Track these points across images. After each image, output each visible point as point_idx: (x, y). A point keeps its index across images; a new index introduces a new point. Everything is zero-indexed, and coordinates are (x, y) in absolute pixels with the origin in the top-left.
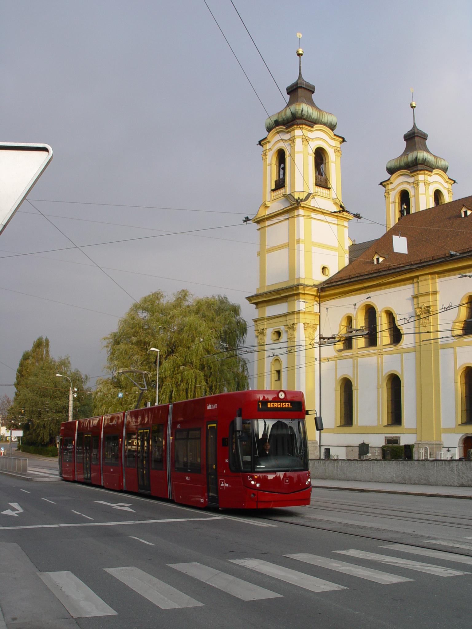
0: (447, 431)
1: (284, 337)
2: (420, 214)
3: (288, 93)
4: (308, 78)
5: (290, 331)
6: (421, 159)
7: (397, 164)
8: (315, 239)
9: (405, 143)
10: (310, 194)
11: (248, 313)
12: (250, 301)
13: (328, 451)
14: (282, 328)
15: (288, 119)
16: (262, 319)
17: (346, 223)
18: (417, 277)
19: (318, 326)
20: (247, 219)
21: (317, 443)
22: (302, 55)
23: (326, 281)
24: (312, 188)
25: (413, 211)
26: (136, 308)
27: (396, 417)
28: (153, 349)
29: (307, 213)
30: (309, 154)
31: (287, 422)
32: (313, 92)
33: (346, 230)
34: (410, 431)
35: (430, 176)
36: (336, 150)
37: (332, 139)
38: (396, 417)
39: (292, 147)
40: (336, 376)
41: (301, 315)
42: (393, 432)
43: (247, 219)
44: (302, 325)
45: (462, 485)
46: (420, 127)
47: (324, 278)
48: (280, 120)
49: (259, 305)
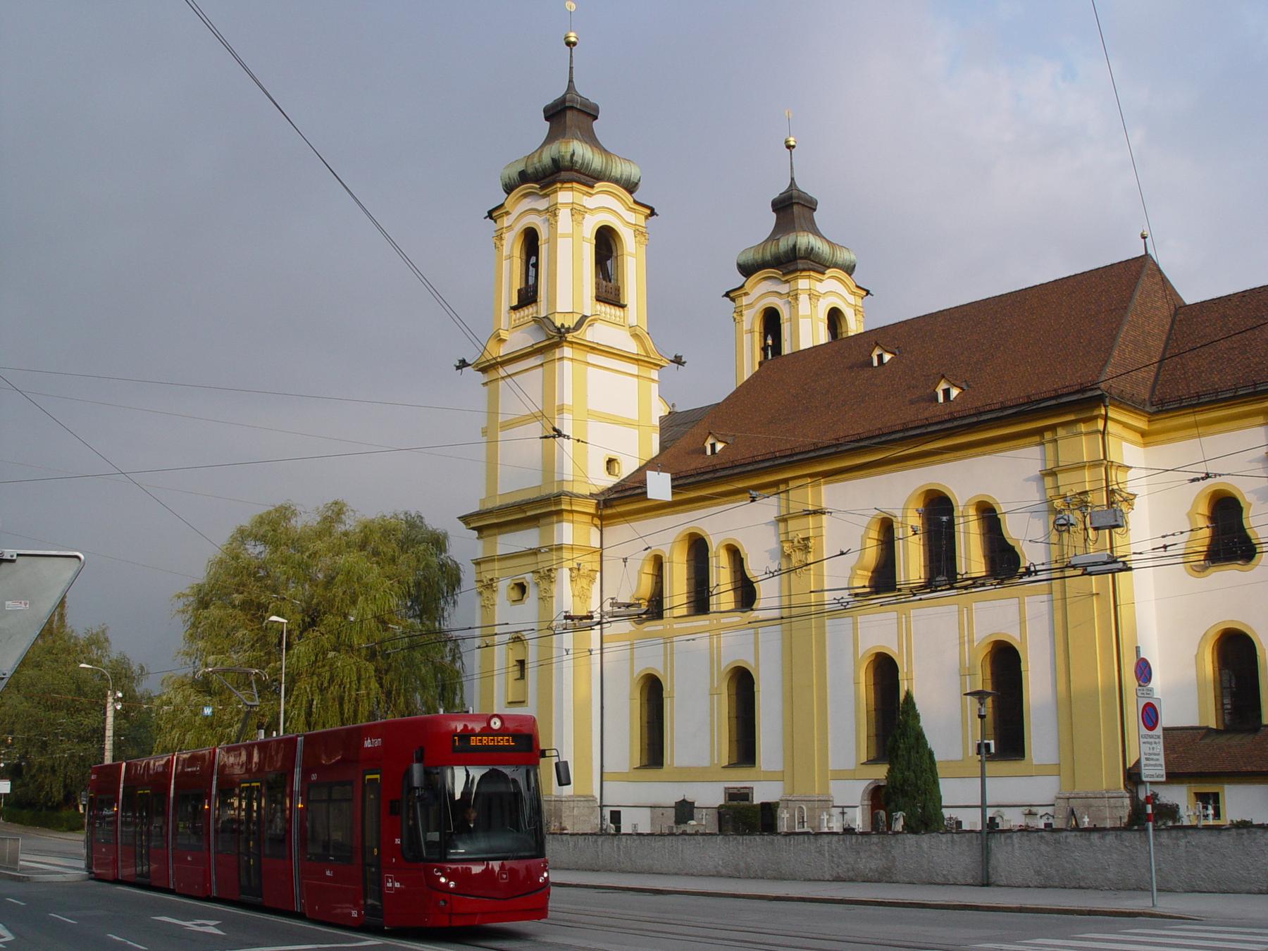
0: (840, 775)
1: (532, 592)
2: (800, 355)
3: (547, 119)
4: (587, 91)
5: (544, 585)
6: (803, 248)
7: (759, 257)
9: (774, 215)
10: (584, 317)
11: (464, 547)
12: (467, 523)
13: (616, 817)
14: (529, 578)
15: (544, 170)
16: (490, 560)
17: (654, 374)
18: (786, 481)
21: (595, 800)
22: (574, 44)
23: (615, 486)
24: (589, 305)
25: (786, 349)
26: (243, 535)
27: (745, 749)
28: (274, 618)
29: (579, 355)
30: (583, 239)
31: (507, 770)
32: (596, 118)
33: (655, 387)
34: (770, 777)
35: (821, 281)
36: (638, 232)
37: (631, 209)
38: (745, 749)
39: (553, 226)
40: (632, 673)
42: (740, 779)
43: (463, 364)
44: (566, 573)
45: (838, 879)
46: (802, 186)
47: (610, 481)
48: (530, 170)
49: (485, 533)
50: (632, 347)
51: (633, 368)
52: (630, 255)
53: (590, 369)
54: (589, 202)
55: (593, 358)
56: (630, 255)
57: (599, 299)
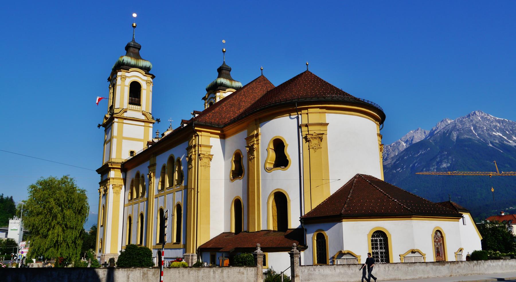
4: (138, 41)
8: (124, 135)
17: (151, 125)
19: (123, 186)
22: (135, 27)
30: (125, 86)
36: (147, 82)
41: (111, 180)
43: (99, 126)
44: (111, 187)
47: (132, 157)
50: (143, 118)
51: (143, 124)
53: (124, 125)
54: (127, 74)
55: (125, 121)
57: (130, 103)
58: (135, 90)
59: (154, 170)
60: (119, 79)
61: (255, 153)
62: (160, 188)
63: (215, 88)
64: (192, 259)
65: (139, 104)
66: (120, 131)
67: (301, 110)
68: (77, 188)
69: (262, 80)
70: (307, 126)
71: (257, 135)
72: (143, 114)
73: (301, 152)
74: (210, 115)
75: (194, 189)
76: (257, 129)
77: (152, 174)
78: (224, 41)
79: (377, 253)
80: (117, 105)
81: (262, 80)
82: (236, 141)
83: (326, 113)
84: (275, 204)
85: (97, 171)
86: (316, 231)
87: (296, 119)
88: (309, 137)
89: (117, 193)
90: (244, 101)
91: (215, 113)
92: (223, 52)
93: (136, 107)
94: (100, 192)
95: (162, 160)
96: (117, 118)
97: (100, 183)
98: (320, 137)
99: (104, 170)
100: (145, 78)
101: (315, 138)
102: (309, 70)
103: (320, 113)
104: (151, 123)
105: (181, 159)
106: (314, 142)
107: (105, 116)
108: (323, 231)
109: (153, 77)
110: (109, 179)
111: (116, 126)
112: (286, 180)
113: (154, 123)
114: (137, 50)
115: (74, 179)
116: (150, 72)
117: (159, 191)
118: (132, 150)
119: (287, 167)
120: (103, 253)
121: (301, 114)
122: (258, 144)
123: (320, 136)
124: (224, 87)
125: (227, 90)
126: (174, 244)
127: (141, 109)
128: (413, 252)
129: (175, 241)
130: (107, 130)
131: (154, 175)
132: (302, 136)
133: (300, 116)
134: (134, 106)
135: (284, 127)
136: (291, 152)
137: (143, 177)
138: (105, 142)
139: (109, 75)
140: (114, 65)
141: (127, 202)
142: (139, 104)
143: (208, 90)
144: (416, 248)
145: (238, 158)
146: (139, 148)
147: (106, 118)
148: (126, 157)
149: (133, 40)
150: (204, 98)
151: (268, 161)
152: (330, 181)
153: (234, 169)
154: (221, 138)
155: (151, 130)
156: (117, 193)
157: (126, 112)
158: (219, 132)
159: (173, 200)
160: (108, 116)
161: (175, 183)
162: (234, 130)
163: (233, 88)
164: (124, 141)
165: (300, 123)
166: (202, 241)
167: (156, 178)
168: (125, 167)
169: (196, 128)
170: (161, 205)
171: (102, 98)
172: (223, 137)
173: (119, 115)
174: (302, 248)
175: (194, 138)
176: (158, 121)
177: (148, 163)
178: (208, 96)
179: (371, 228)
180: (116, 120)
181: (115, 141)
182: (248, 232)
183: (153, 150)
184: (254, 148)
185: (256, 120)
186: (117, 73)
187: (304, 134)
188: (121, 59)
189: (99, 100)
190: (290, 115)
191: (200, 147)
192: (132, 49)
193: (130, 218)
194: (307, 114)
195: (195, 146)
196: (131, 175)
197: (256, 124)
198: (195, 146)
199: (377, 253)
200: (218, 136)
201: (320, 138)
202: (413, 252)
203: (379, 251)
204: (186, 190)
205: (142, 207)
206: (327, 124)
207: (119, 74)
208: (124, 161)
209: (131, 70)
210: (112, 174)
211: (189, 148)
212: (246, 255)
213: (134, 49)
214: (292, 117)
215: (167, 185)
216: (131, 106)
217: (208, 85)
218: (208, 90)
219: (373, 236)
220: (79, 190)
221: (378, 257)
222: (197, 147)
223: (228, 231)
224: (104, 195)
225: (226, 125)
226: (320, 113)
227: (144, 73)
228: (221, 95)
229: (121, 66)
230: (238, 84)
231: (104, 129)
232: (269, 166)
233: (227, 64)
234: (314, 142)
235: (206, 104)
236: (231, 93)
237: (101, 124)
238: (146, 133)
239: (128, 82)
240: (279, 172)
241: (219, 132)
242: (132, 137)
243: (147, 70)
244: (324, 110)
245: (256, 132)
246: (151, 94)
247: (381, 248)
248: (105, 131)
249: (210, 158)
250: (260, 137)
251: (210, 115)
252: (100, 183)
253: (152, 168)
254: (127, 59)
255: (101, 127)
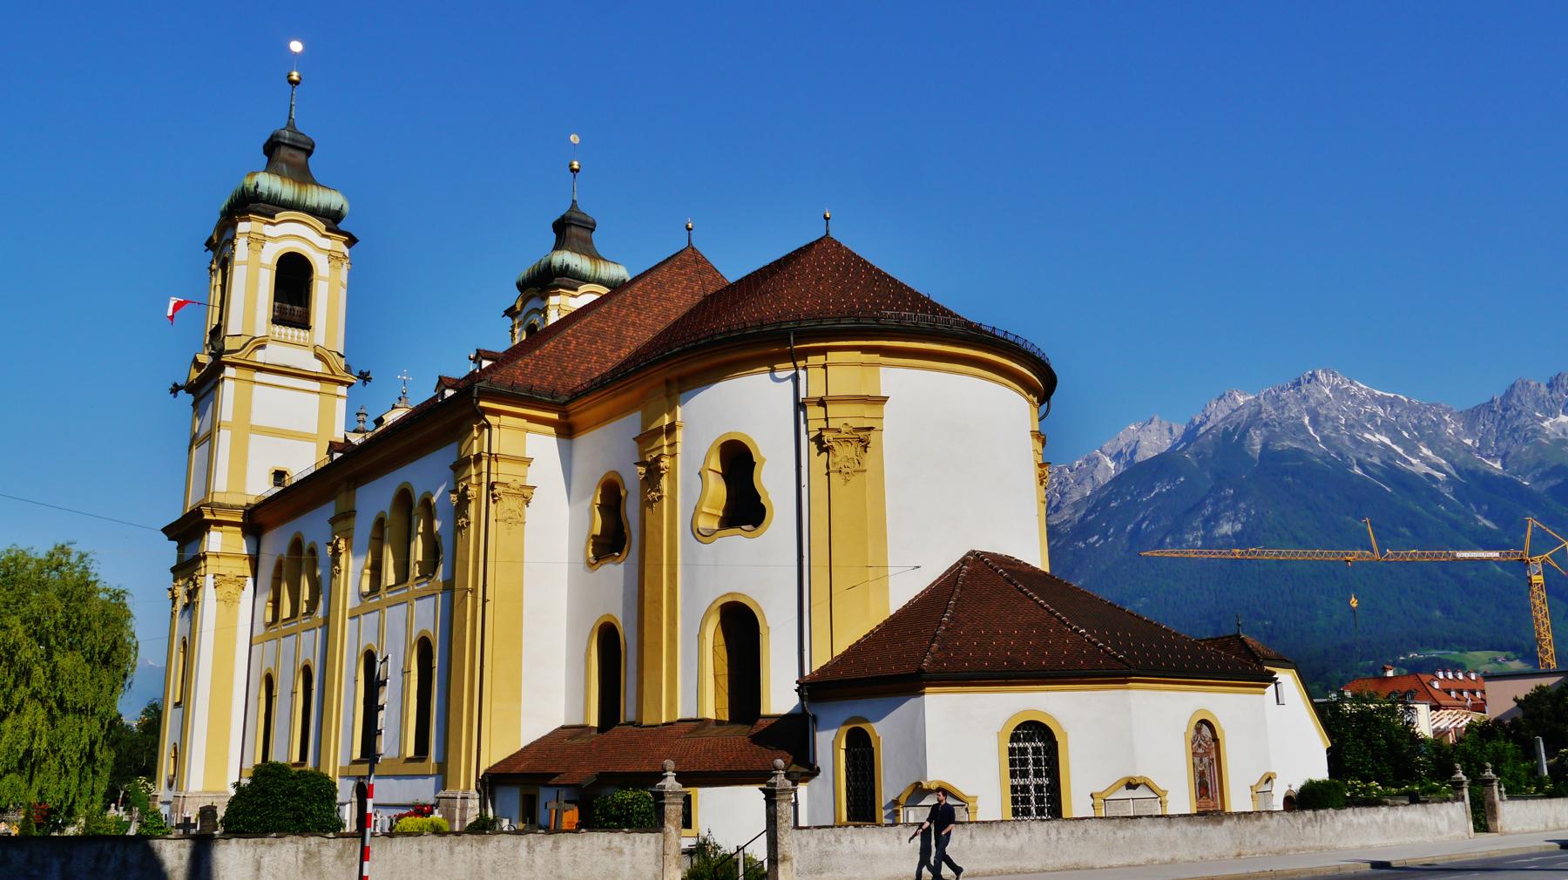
4: (307, 128)
8: (257, 419)
17: (342, 390)
19: (250, 581)
20: (175, 389)
22: (297, 83)
29: (244, 374)
30: (262, 265)
33: (343, 402)
36: (332, 257)
43: (175, 389)
47: (278, 489)
50: (317, 367)
51: (316, 386)
52: (323, 279)
53: (257, 387)
54: (268, 230)
55: (259, 377)
56: (323, 279)
57: (276, 321)
58: (293, 279)
59: (350, 529)
60: (241, 244)
61: (664, 482)
62: (366, 588)
63: (544, 281)
64: (464, 809)
65: (303, 323)
66: (243, 406)
67: (805, 354)
68: (100, 586)
69: (688, 260)
70: (822, 403)
71: (671, 429)
72: (318, 356)
73: (804, 481)
74: (527, 365)
75: (474, 591)
76: (671, 410)
77: (342, 544)
78: (574, 139)
79: (1025, 789)
80: (234, 326)
81: (688, 260)
82: (608, 445)
83: (880, 364)
84: (721, 640)
85: (165, 530)
86: (845, 724)
87: (790, 383)
88: (827, 436)
89: (229, 602)
90: (634, 324)
91: (541, 358)
92: (573, 170)
93: (296, 332)
94: (174, 599)
95: (375, 499)
96: (233, 365)
97: (173, 570)
98: (863, 438)
99: (188, 530)
100: (327, 244)
101: (846, 441)
102: (831, 235)
103: (862, 364)
104: (342, 383)
105: (434, 499)
106: (844, 453)
107: (195, 360)
108: (866, 721)
109: (351, 241)
110: (205, 558)
111: (230, 388)
112: (758, 568)
113: (350, 385)
114: (301, 157)
115: (91, 556)
116: (341, 226)
117: (363, 596)
118: (281, 467)
119: (760, 529)
120: (179, 789)
121: (805, 368)
122: (673, 455)
123: (861, 435)
124: (571, 279)
125: (582, 288)
126: (409, 760)
127: (311, 338)
128: (1131, 785)
129: (410, 752)
130: (201, 403)
131: (349, 547)
132: (807, 433)
133: (802, 373)
134: (290, 331)
135: (750, 405)
136: (774, 481)
137: (313, 551)
138: (195, 440)
139: (209, 229)
140: (227, 201)
141: (259, 629)
142: (303, 323)
143: (522, 286)
144: (1138, 773)
145: (611, 497)
146: (303, 461)
147: (198, 365)
148: (260, 487)
149: (291, 125)
150: (511, 312)
151: (705, 509)
152: (891, 571)
153: (597, 531)
154: (559, 435)
155: (341, 405)
156: (229, 602)
157: (262, 347)
158: (555, 416)
159: (408, 625)
160: (205, 359)
161: (415, 571)
162: (601, 410)
163: (600, 282)
164: (254, 438)
165: (803, 395)
166: (493, 755)
167: (356, 555)
168: (255, 521)
169: (482, 404)
170: (368, 640)
171: (186, 302)
172: (566, 431)
173: (238, 357)
174: (803, 774)
175: (476, 433)
176: (365, 377)
177: (329, 510)
178: (523, 306)
179: (1009, 714)
180: (229, 371)
181: (224, 439)
182: (640, 725)
183: (347, 469)
184: (659, 469)
185: (668, 382)
186: (235, 226)
187: (815, 426)
188: (250, 183)
189: (177, 306)
190: (773, 370)
191: (493, 463)
192: (284, 153)
193: (269, 682)
194: (825, 366)
195: (478, 458)
196: (275, 545)
197: (668, 396)
198: (478, 458)
199: (1025, 789)
200: (552, 430)
201: (861, 441)
202: (1131, 785)
203: (1032, 781)
204: (448, 594)
205: (308, 645)
206: (884, 400)
207: (243, 227)
208: (252, 501)
209: (280, 216)
210: (214, 541)
211: (461, 465)
212: (630, 795)
213: (292, 152)
214: (778, 375)
215: (390, 577)
216: (277, 328)
217: (523, 272)
218: (522, 286)
219: (1014, 738)
220: (106, 590)
221: (1029, 802)
222: (485, 463)
223: (577, 721)
224: (186, 607)
225: (576, 395)
226: (862, 364)
227: (322, 227)
228: (561, 305)
229: (247, 204)
230: (619, 272)
231: (190, 398)
232: (707, 523)
233: (582, 207)
234: (844, 453)
235: (517, 331)
236: (596, 297)
237: (182, 382)
238: (325, 416)
239: (271, 254)
240: (737, 542)
241: (555, 416)
242: (280, 428)
243: (331, 219)
244: (876, 358)
245: (667, 420)
246: (343, 293)
247: (1037, 774)
248: (194, 405)
249: (525, 495)
250: (679, 434)
251: (527, 365)
252: (173, 570)
253: (342, 525)
254: (269, 183)
255: (182, 393)
